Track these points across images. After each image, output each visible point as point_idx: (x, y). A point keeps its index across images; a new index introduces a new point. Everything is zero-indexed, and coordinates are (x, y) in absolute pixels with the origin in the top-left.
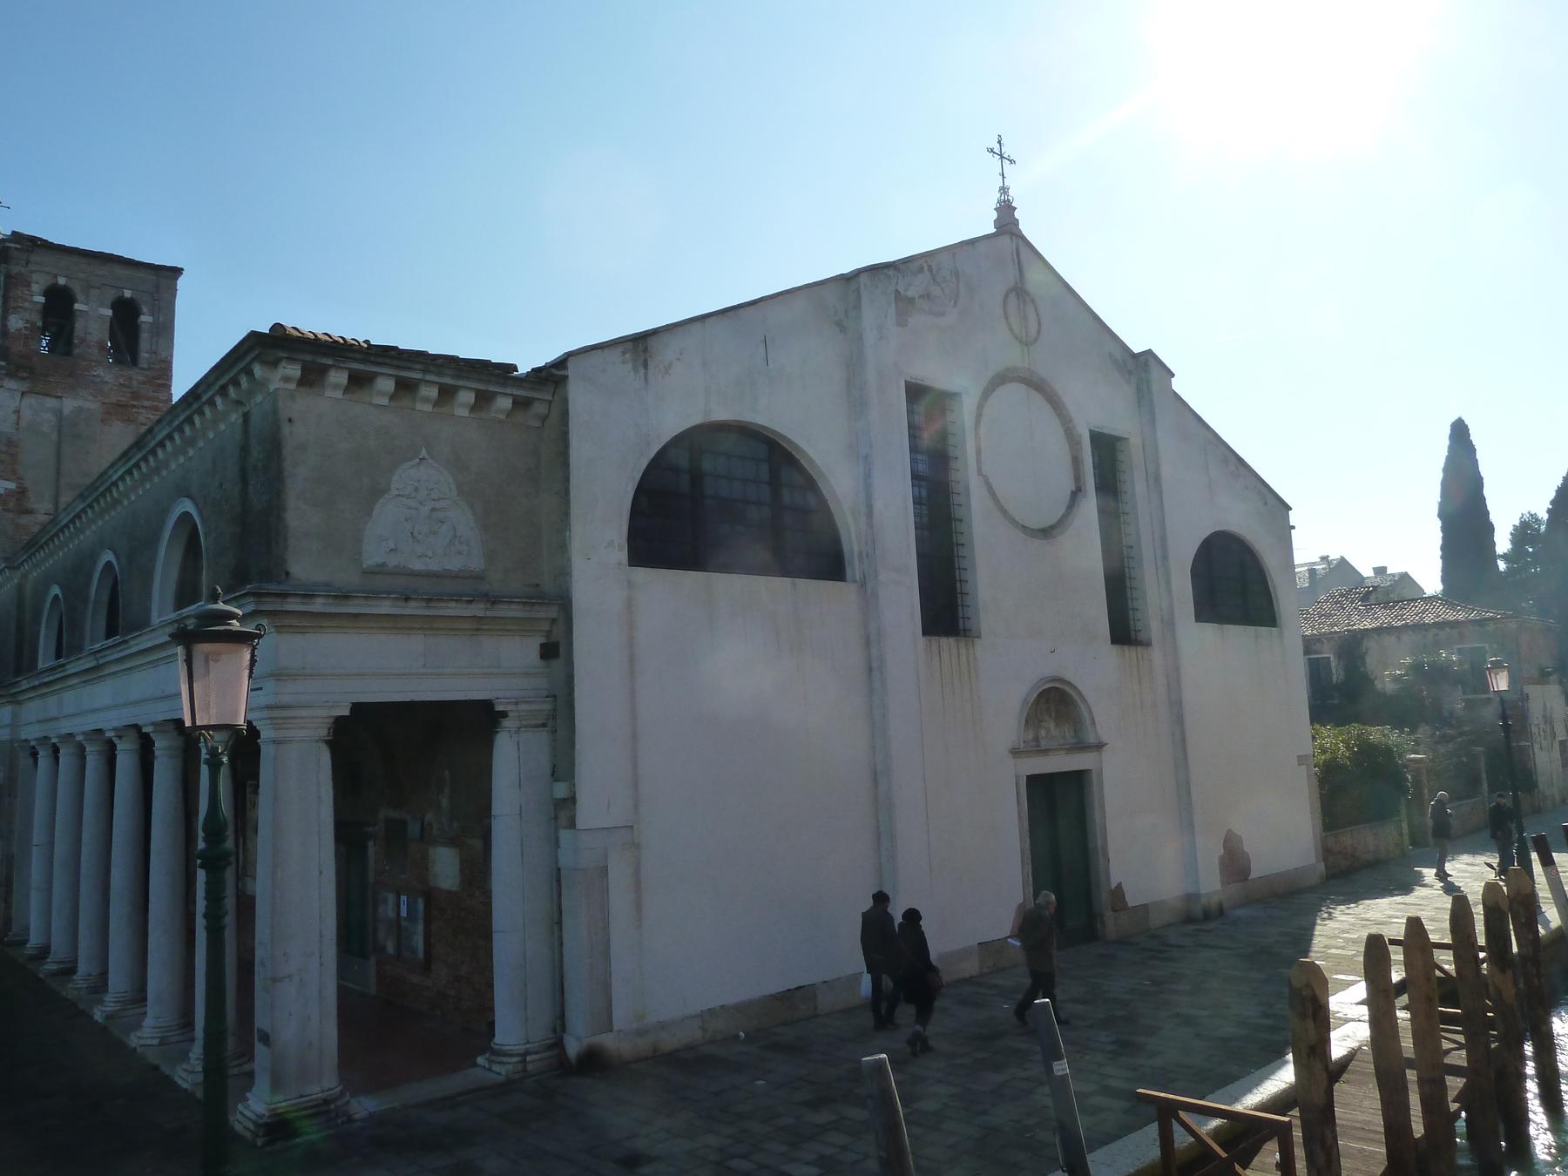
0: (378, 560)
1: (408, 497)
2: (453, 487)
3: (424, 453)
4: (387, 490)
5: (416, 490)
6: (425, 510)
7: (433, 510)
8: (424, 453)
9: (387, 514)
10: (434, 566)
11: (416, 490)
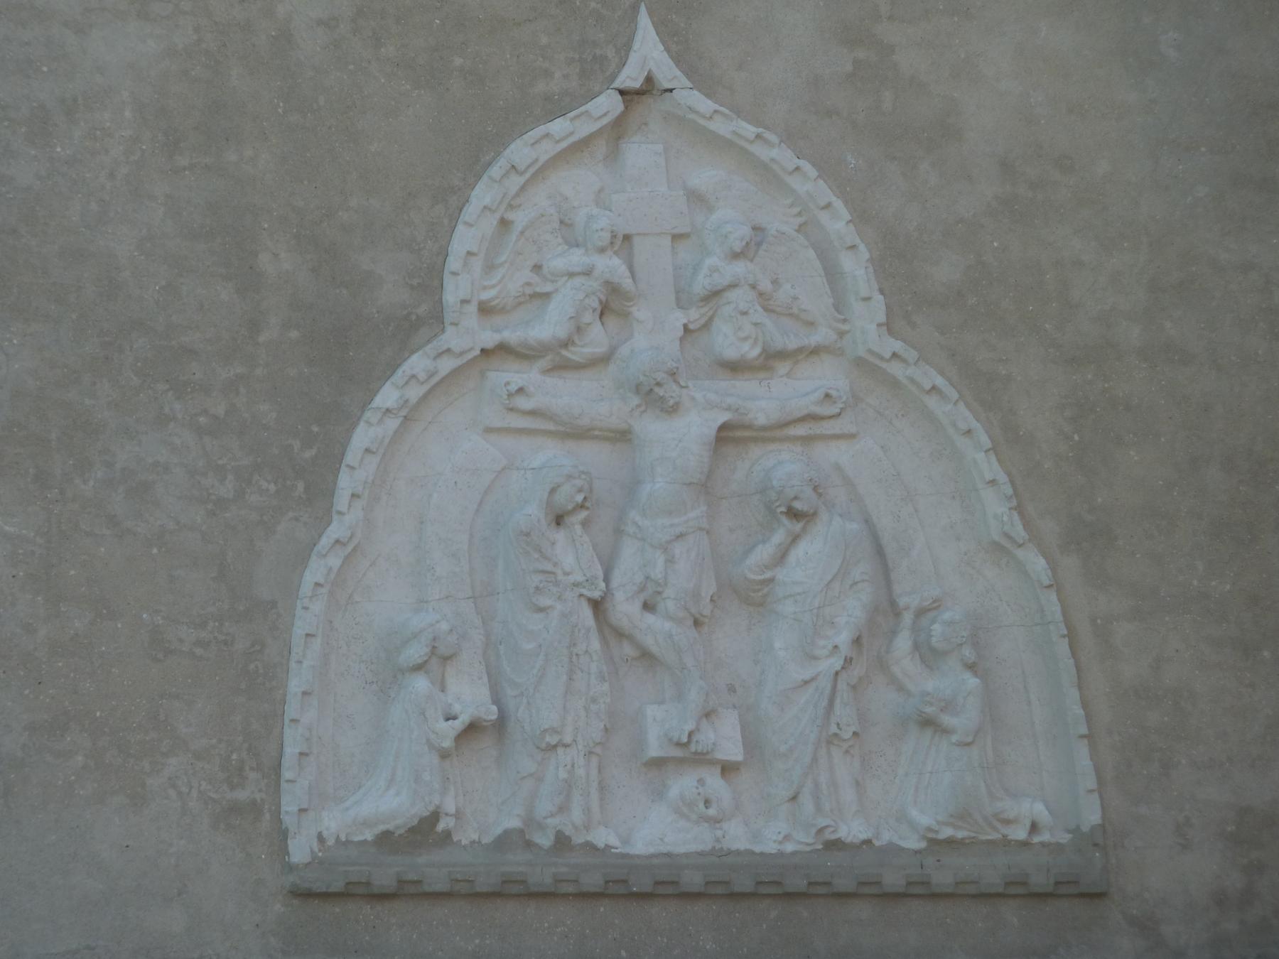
0: (385, 802)
1: (559, 358)
2: (856, 268)
3: (648, 53)
4: (419, 320)
5: (612, 304)
6: (681, 437)
7: (729, 436)
8: (648, 53)
9: (433, 482)
10: (767, 830)
11: (612, 304)
